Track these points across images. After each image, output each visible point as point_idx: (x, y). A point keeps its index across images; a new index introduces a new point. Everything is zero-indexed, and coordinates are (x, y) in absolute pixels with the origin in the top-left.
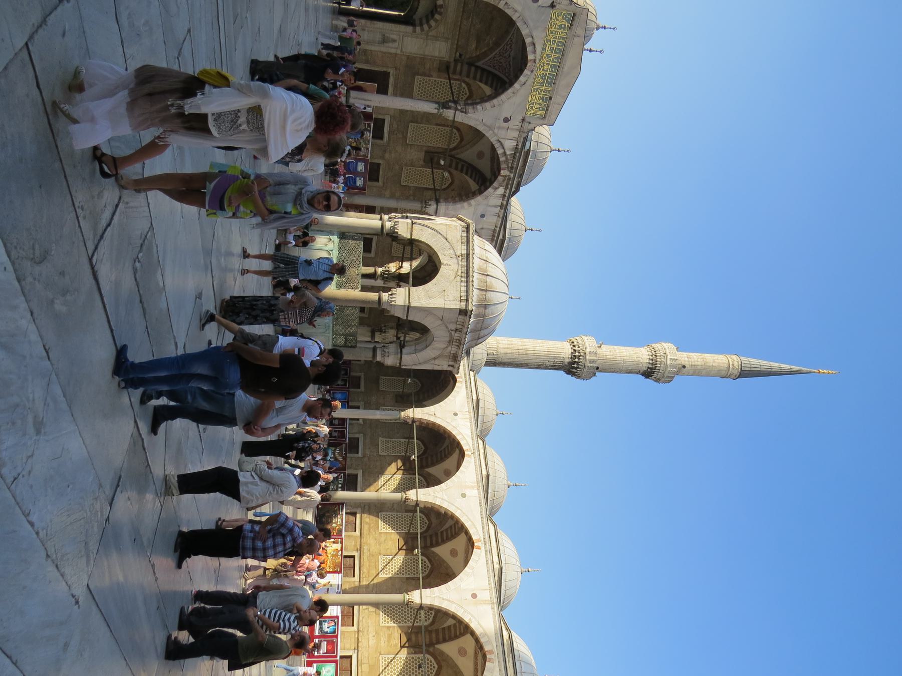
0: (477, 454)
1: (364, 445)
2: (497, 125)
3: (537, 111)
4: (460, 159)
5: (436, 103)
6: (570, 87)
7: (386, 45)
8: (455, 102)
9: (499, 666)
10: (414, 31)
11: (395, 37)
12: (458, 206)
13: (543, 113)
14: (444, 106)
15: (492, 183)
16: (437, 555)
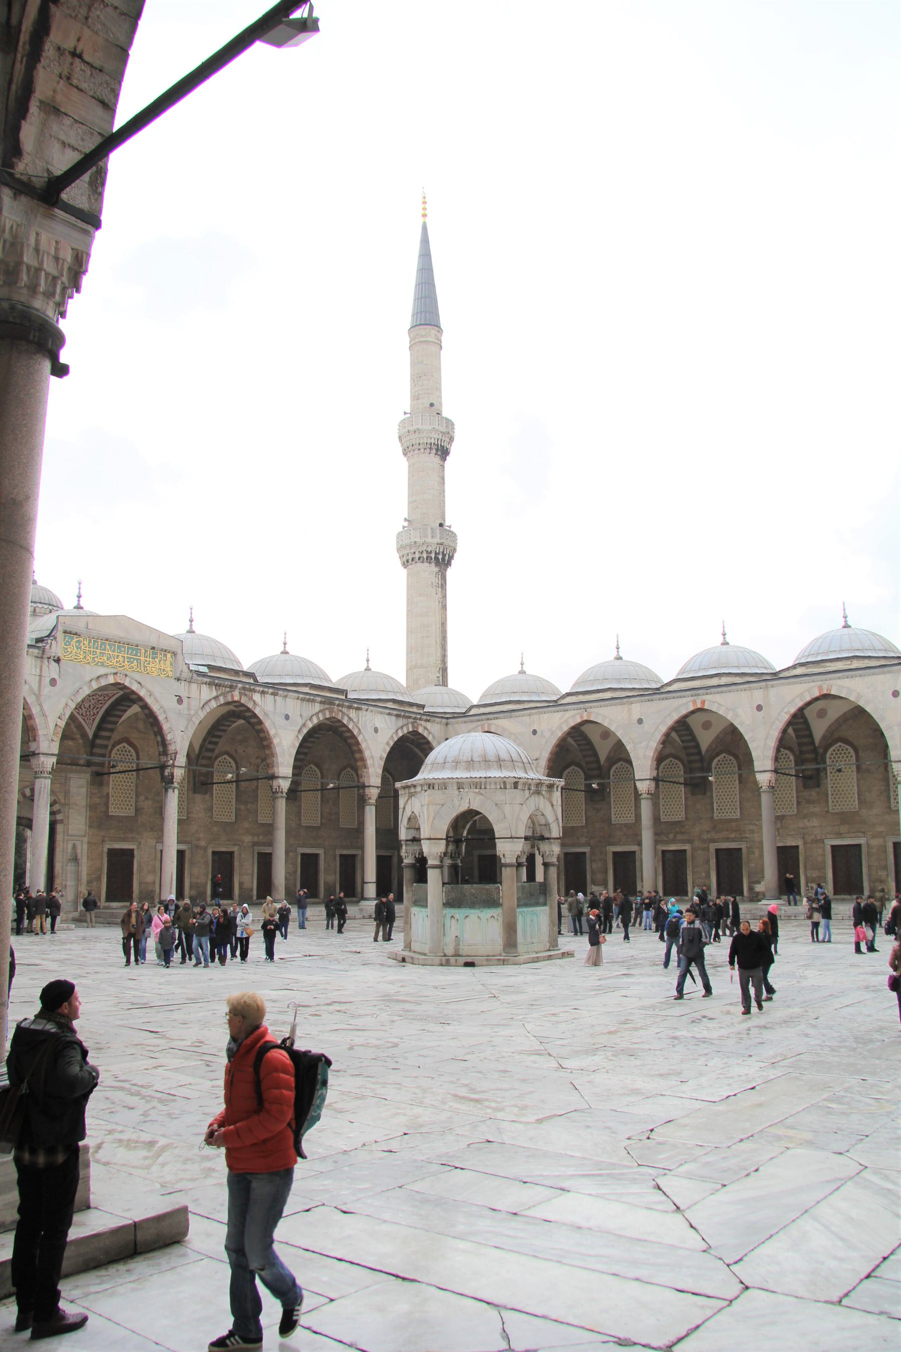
0: (587, 705)
1: (574, 845)
2: (186, 712)
3: (168, 663)
4: (201, 747)
5: (166, 790)
6: (139, 626)
7: (79, 856)
8: (163, 767)
9: (834, 679)
10: (62, 821)
11: (70, 846)
12: (278, 750)
13: (169, 655)
14: (168, 781)
15: (249, 710)
16: (710, 746)
